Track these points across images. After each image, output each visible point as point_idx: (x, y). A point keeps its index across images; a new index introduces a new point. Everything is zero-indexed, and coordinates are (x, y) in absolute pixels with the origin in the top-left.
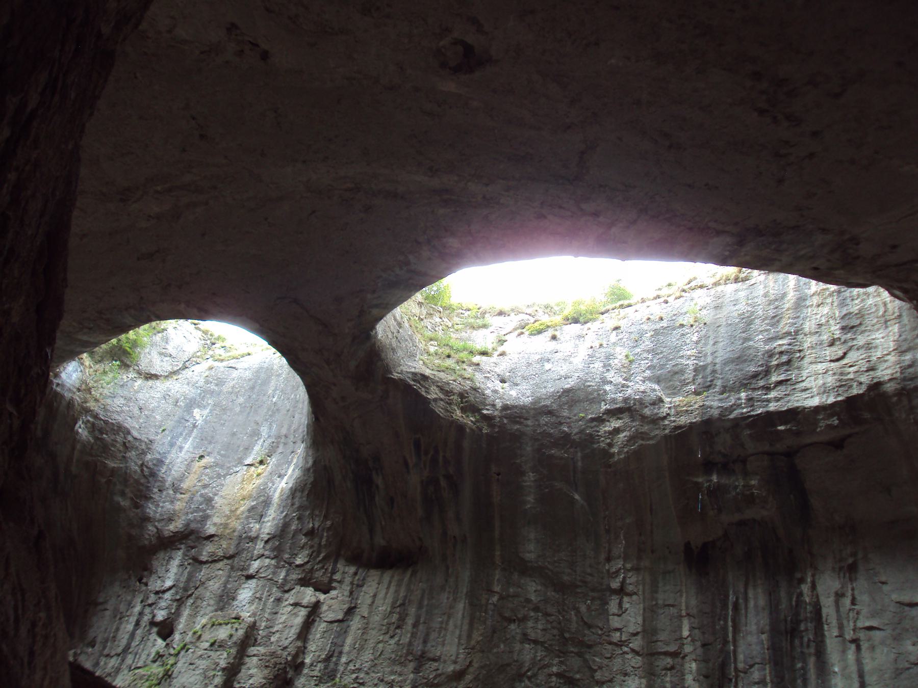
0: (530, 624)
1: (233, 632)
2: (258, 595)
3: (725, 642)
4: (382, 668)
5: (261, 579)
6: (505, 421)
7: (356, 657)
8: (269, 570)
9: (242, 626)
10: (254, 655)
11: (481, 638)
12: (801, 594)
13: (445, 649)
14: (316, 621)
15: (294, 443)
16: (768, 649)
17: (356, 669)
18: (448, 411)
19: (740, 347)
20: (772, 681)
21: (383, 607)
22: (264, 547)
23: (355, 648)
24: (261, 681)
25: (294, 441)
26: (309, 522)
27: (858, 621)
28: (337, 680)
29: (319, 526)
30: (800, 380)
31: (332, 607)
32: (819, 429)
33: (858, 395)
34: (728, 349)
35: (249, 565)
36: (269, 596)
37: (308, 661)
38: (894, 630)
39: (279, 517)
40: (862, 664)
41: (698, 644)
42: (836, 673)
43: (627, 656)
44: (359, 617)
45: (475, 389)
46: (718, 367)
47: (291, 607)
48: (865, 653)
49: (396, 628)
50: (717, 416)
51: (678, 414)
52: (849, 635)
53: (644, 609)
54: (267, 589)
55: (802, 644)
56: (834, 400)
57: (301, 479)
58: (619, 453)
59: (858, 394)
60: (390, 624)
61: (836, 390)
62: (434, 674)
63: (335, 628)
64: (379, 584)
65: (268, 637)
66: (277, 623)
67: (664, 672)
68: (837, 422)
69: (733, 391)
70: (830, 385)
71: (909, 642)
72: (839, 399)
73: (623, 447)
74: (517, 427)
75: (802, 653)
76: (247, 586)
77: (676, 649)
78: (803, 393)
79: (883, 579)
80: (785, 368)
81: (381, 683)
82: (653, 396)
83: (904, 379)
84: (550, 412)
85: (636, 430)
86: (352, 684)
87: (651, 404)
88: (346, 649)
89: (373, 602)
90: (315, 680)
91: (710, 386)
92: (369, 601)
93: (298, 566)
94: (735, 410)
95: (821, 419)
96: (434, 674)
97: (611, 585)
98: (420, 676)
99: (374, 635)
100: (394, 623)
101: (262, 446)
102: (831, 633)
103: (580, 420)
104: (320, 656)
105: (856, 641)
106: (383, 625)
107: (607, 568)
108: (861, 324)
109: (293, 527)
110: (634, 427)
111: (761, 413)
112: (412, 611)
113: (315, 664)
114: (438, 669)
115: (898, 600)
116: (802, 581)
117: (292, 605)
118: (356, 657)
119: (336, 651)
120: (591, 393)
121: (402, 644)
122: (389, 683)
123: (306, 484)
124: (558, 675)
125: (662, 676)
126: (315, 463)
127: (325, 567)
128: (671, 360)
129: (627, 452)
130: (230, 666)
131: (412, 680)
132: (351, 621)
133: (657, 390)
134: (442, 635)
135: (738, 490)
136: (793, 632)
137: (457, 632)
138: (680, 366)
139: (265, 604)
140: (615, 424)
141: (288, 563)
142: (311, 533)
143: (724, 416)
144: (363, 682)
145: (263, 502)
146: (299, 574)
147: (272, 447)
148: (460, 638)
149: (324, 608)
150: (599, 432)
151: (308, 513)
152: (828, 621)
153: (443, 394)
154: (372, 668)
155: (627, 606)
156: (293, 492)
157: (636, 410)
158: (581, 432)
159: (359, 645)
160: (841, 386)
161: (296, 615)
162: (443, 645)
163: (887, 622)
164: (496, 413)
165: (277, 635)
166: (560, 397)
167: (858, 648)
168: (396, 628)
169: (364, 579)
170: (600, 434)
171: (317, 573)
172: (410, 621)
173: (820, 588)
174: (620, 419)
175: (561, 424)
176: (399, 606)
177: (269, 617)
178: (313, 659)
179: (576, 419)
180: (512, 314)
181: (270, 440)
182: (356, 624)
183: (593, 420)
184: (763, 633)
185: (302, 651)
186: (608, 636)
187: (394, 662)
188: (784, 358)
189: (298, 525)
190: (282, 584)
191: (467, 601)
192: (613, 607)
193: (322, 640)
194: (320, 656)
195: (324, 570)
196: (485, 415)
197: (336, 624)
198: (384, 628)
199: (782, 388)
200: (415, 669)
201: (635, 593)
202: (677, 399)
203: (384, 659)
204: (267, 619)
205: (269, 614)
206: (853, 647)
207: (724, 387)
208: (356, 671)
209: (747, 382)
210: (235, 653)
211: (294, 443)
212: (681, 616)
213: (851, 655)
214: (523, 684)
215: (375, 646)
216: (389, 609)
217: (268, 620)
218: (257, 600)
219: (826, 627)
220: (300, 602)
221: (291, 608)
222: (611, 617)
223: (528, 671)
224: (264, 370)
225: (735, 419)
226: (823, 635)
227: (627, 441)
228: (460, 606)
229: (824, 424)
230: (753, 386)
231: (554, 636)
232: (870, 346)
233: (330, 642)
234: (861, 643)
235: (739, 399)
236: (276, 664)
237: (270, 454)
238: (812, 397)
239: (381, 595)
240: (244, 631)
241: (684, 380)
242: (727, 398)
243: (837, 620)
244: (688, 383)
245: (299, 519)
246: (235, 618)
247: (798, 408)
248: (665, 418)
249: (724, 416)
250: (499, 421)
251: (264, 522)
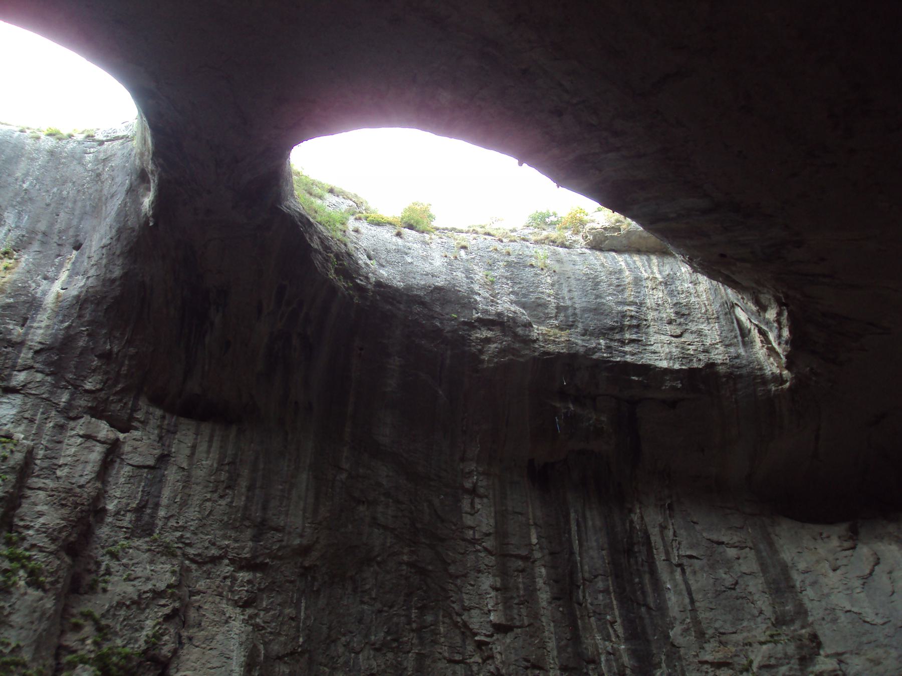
0: (380, 509)
1: (7, 454)
2: (26, 415)
3: (572, 553)
4: (212, 530)
5: (31, 397)
6: (378, 298)
7: (178, 513)
8: (44, 388)
9: (19, 448)
10: (40, 489)
11: (328, 515)
12: (632, 522)
13: (289, 520)
14: (115, 462)
15: (59, 245)
16: (608, 564)
17: (180, 527)
18: (324, 267)
19: (595, 301)
20: (614, 591)
21: (207, 462)
22: (33, 358)
23: (176, 502)
24: (58, 521)
25: (60, 243)
26: (105, 343)
27: (680, 550)
28: (155, 535)
29: (119, 351)
30: (649, 343)
31: (139, 450)
32: (664, 388)
33: (697, 369)
34: (584, 299)
35: (10, 376)
36: (46, 419)
37: (111, 507)
38: (709, 560)
39: (56, 327)
40: (689, 584)
41: (546, 551)
42: (669, 589)
43: (480, 554)
44: (175, 468)
45: (349, 255)
46: (577, 311)
47: (81, 439)
49: (226, 488)
50: (582, 353)
51: (545, 341)
52: (675, 560)
53: (496, 512)
54: (41, 410)
55: (637, 563)
56: (680, 367)
57: (98, 289)
58: (489, 361)
59: (698, 368)
60: (218, 482)
61: (680, 359)
62: (278, 546)
63: (145, 475)
64: (197, 434)
65: (53, 469)
66: (63, 455)
67: (516, 573)
68: (680, 386)
69: (593, 336)
70: (675, 354)
71: (721, 571)
72: (683, 367)
73: (494, 357)
74: (389, 307)
75: (638, 570)
76: (7, 401)
77: (527, 553)
78: (653, 355)
79: (695, 520)
80: (635, 330)
81: (213, 547)
83: (733, 366)
84: (423, 303)
85: (508, 345)
86: (176, 543)
87: (523, 326)
88: (164, 501)
89: (193, 454)
90: (125, 532)
91: (572, 326)
92: (187, 452)
93: (87, 391)
94: (596, 352)
95: (668, 380)
96: (278, 545)
97: (465, 484)
98: (261, 545)
99: (198, 493)
100: (223, 481)
101: (6, 235)
102: (660, 557)
103: (453, 320)
104: (128, 504)
105: (680, 565)
106: (210, 482)
107: (461, 467)
108: (689, 314)
109: (81, 344)
110: (506, 341)
111: (619, 361)
112: (245, 472)
113: (122, 513)
114: (281, 541)
115: (708, 538)
116: (631, 511)
117: (81, 436)
118: (178, 513)
119: (150, 502)
121: (235, 507)
122: (223, 548)
123: (106, 297)
124: (410, 564)
125: (515, 577)
126: (125, 276)
127: (124, 401)
129: (497, 363)
130: (8, 496)
131: (252, 549)
132: (165, 470)
133: (524, 315)
134: (284, 504)
135: (591, 422)
136: (629, 552)
137: (302, 504)
139: (40, 428)
140: (489, 334)
141: (72, 385)
142: (106, 357)
143: (589, 355)
144: (191, 543)
145: (25, 302)
146: (89, 401)
147: (21, 240)
148: (304, 511)
149: (126, 448)
150: (470, 336)
151: (104, 331)
152: (657, 547)
153: (322, 247)
154: (201, 528)
155: (479, 507)
156: (82, 301)
157: (509, 326)
158: (454, 331)
159: (181, 498)
160: (684, 358)
161: (90, 450)
162: (287, 515)
163: (702, 553)
164: (369, 287)
165: (66, 470)
166: (432, 292)
167: (683, 572)
168: (226, 488)
169: (176, 426)
170: (471, 338)
171: (113, 405)
172: (243, 483)
173: (647, 519)
174: (491, 330)
175: (434, 318)
176: (228, 464)
177: (50, 446)
178: (119, 506)
179: (448, 318)
180: (341, 197)
181: (19, 232)
182: (172, 475)
183: (464, 323)
184: (603, 550)
185: (101, 495)
186: (461, 532)
187: (225, 525)
188: (635, 322)
189: (88, 342)
190: (65, 408)
191: (311, 473)
192: (466, 504)
193: (129, 485)
194: (128, 504)
195: (122, 405)
196: (358, 284)
197: (146, 470)
198: (211, 485)
200: (254, 536)
201: (486, 497)
202: (543, 329)
203: (214, 520)
204: (46, 447)
205: (48, 441)
206: (679, 570)
207: (586, 330)
208: (181, 530)
209: (607, 332)
210: (14, 480)
211: (59, 245)
212: (529, 525)
214: (372, 569)
215: (202, 504)
216: (215, 465)
217: (47, 448)
218: (26, 421)
219: (655, 551)
220: (96, 435)
221: (80, 440)
222: (463, 515)
223: (378, 556)
224: (11, 146)
225: (597, 360)
226: (653, 558)
227: (498, 352)
228: (304, 476)
229: (669, 385)
230: (610, 337)
231: (405, 524)
232: (701, 333)
233: (141, 489)
234: (685, 568)
235: (599, 344)
236: (77, 504)
237: (16, 249)
238: (661, 360)
239: (202, 447)
240: (24, 455)
241: (548, 313)
242: (588, 340)
243: (664, 547)
244: (551, 318)
245: (88, 335)
246: (6, 437)
247: (651, 365)
248: (535, 341)
249: (589, 355)
250: (372, 296)
251: (32, 327)
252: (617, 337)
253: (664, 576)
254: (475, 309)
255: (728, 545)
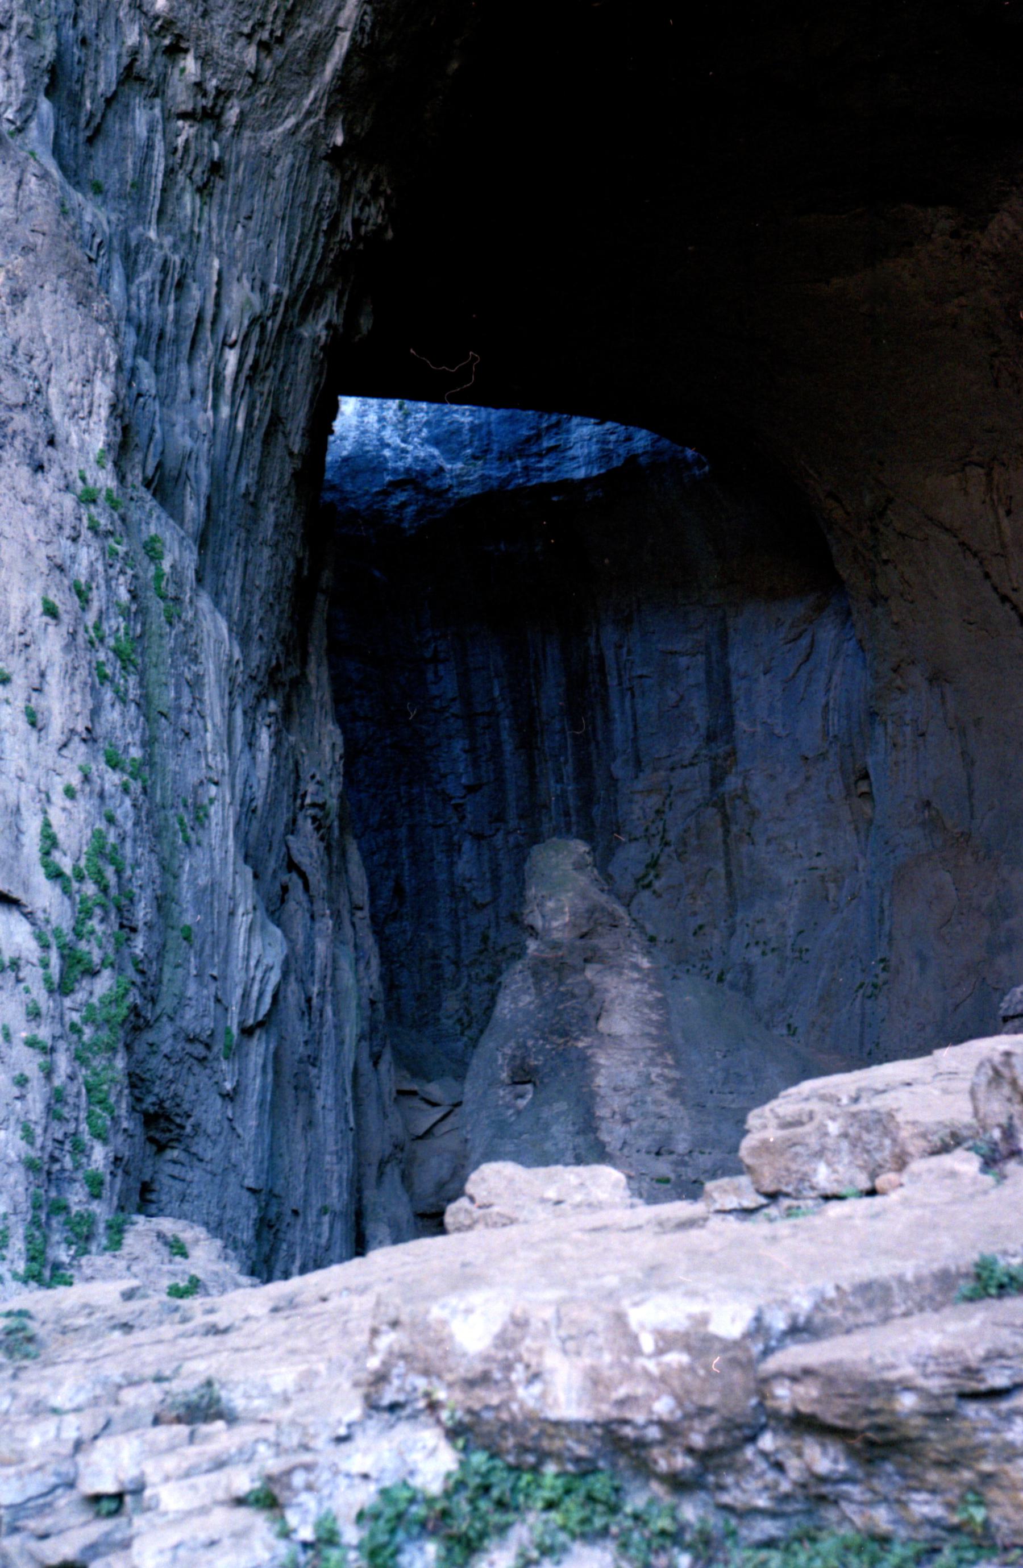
48: (639, 701)
51: (462, 485)
52: (626, 685)
82: (433, 464)
102: (612, 681)
120: (371, 461)
128: (446, 414)
138: (456, 425)
140: (402, 497)
166: (340, 468)
167: (633, 696)
175: (346, 500)
183: (378, 493)
199: (553, 455)
206: (629, 693)
207: (501, 453)
213: (628, 704)
235: (515, 467)
252: (534, 449)
253: (614, 704)
254: (386, 469)
255: (682, 654)
